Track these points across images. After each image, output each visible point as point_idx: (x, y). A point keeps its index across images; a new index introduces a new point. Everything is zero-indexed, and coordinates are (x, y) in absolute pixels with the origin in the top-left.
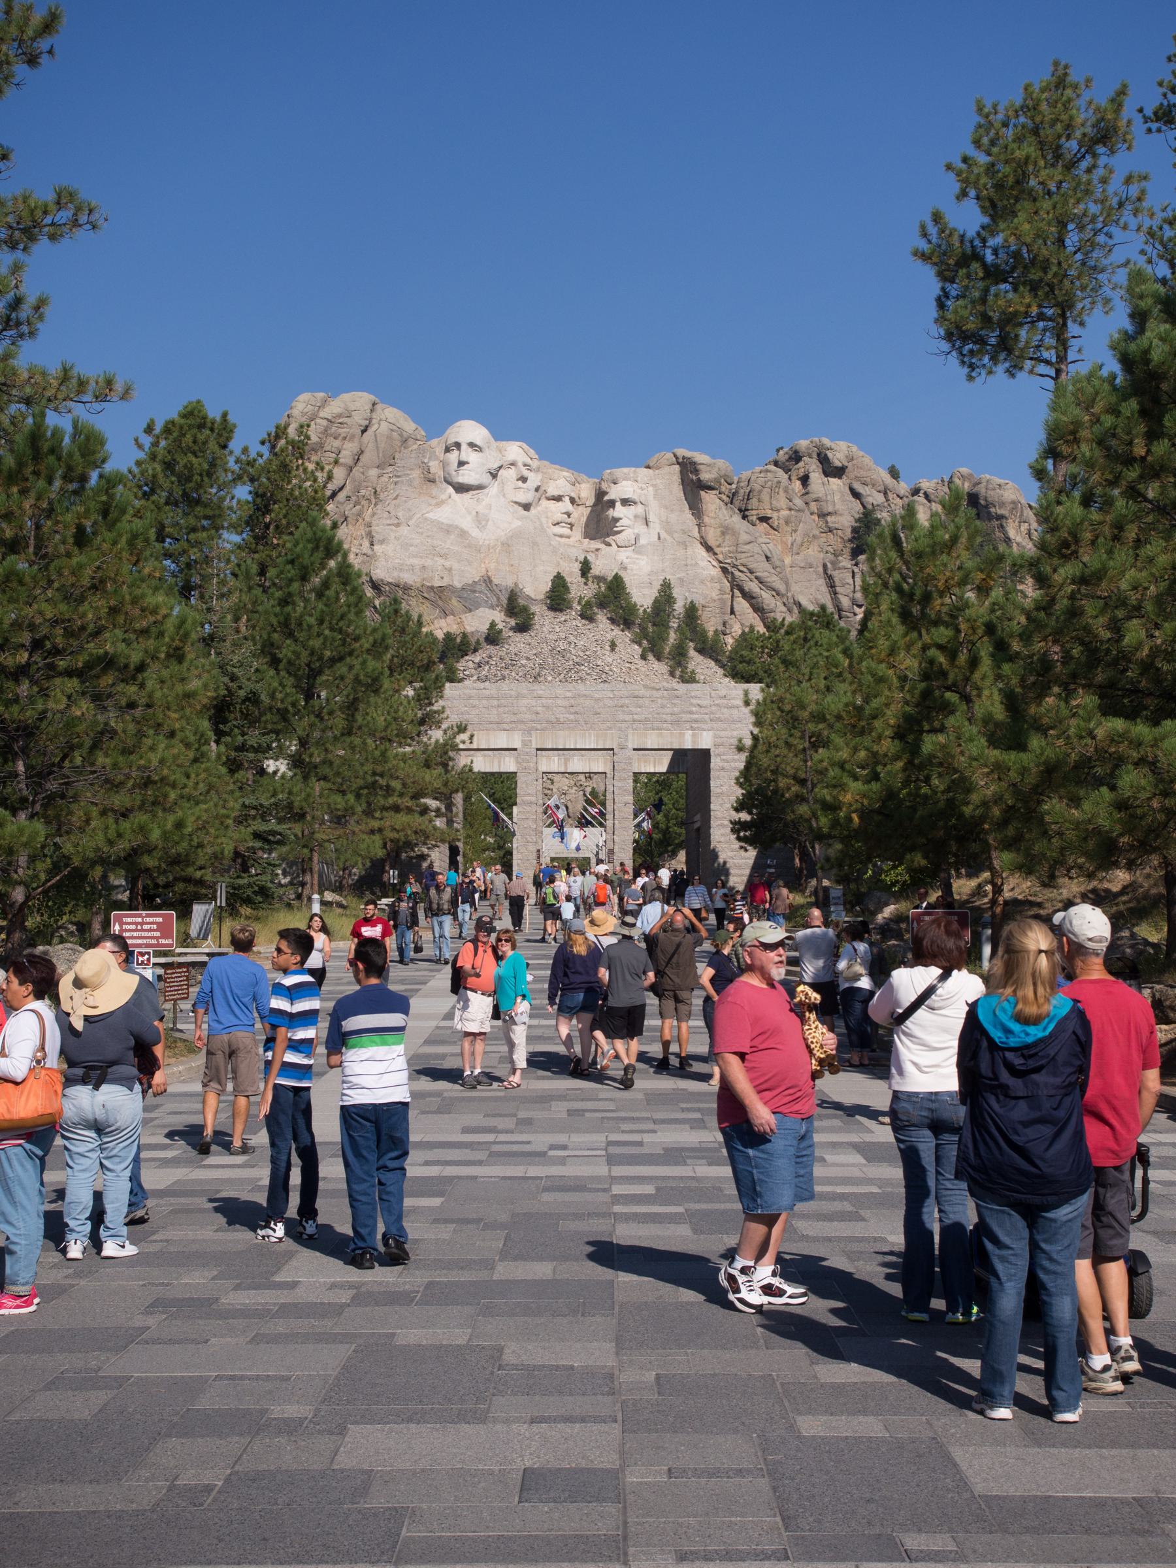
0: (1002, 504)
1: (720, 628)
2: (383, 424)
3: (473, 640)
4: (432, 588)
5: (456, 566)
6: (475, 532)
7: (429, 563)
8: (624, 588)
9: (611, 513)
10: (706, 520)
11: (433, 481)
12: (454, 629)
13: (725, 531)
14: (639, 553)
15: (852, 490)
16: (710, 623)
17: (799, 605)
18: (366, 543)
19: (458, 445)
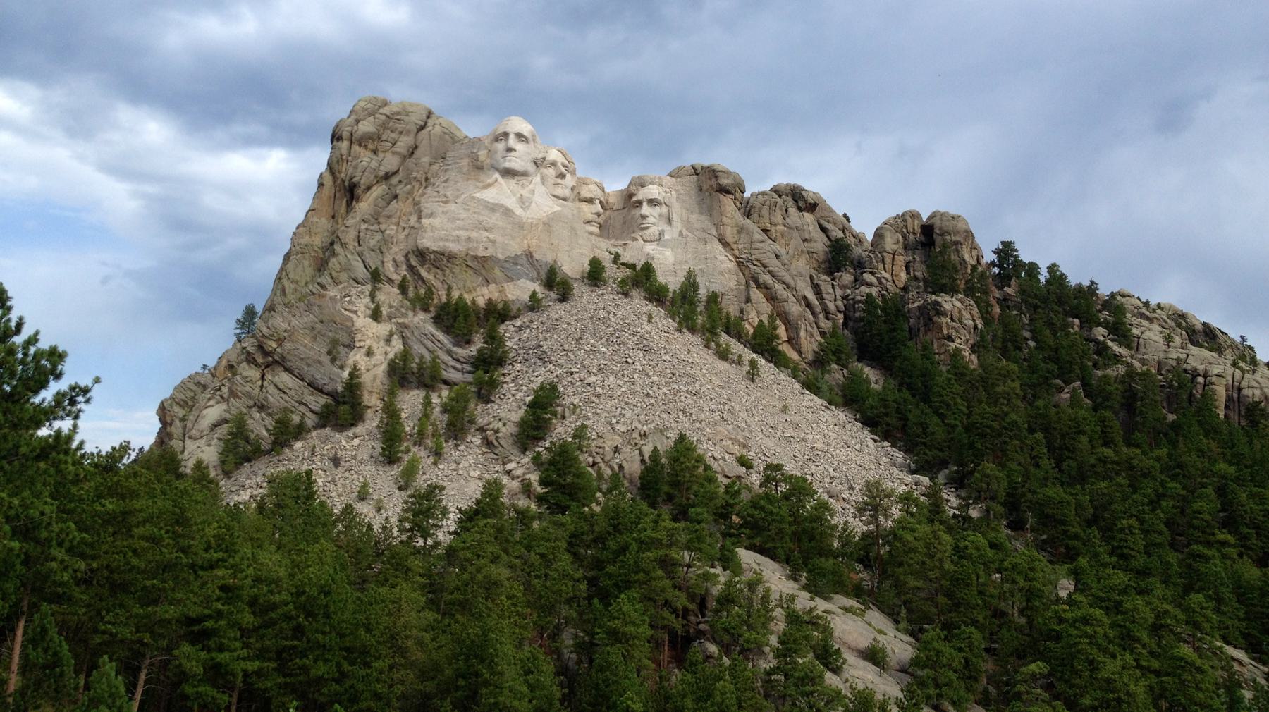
0: (957, 233)
1: (738, 314)
3: (514, 308)
4: (476, 258)
5: (500, 239)
7: (474, 235)
8: (654, 271)
9: (636, 212)
10: (725, 219)
11: (479, 168)
12: (495, 296)
13: (741, 230)
15: (820, 225)
16: (731, 307)
17: (805, 298)
18: (413, 219)
19: (506, 135)
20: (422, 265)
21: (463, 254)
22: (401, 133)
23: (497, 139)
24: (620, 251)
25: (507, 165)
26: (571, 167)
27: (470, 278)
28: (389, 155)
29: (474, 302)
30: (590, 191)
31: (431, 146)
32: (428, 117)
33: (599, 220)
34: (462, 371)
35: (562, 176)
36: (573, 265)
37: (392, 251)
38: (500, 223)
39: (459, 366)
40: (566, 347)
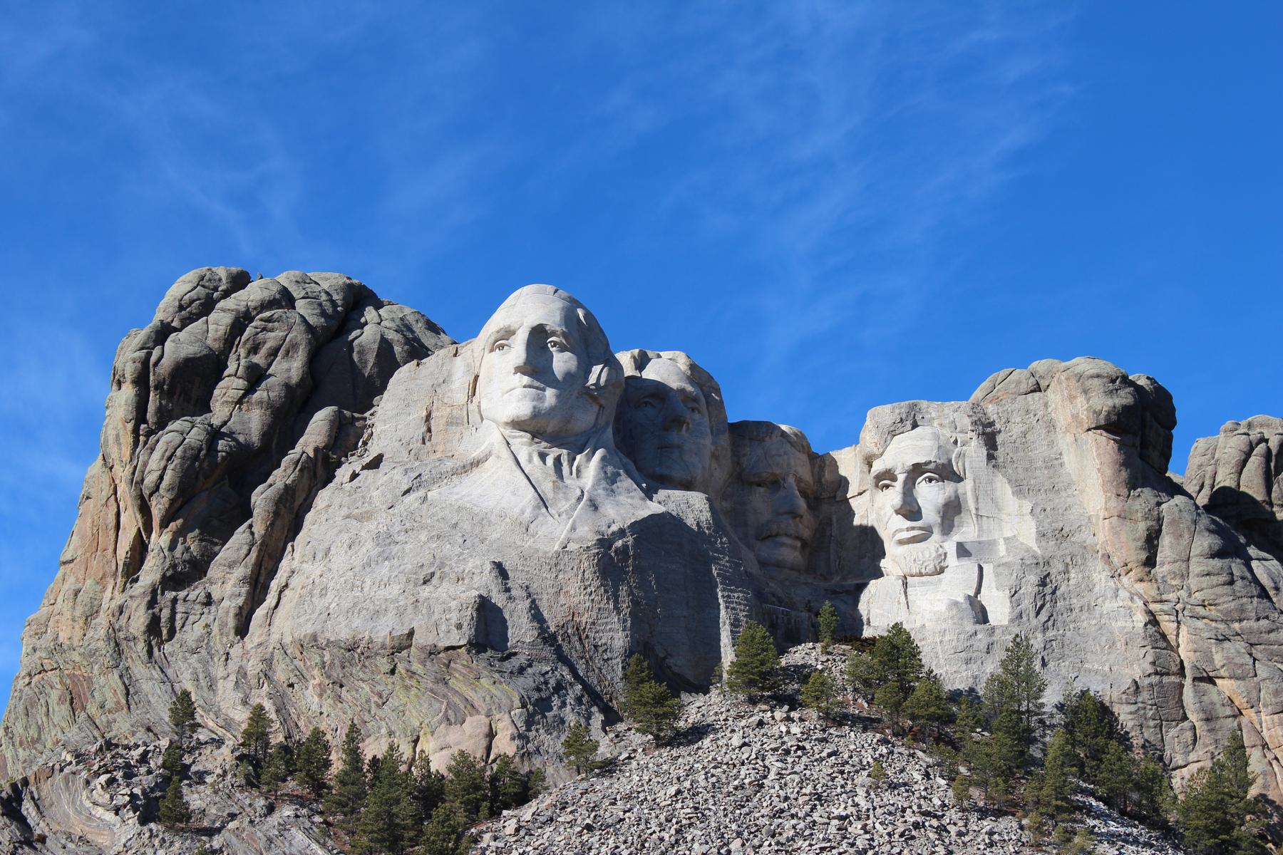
4: (433, 652)
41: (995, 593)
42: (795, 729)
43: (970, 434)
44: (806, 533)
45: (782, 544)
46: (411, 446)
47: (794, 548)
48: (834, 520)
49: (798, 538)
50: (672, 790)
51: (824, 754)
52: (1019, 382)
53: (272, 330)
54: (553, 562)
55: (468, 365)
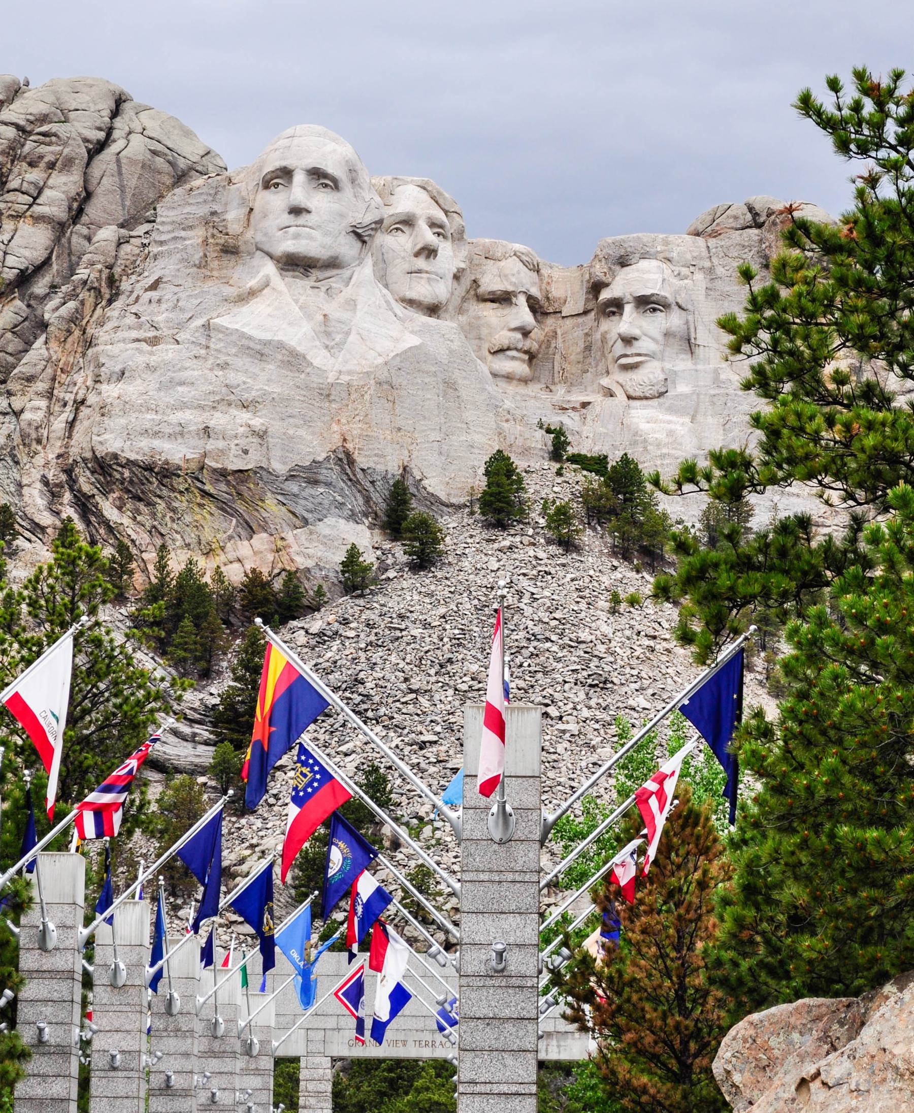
2: (136, 139)
3: (309, 587)
4: (223, 474)
5: (276, 428)
6: (319, 358)
7: (218, 420)
11: (230, 251)
14: (671, 410)
20: (105, 494)
21: (194, 466)
22: (51, 166)
23: (267, 184)
24: (570, 422)
25: (288, 246)
26: (451, 226)
27: (214, 525)
28: (25, 227)
29: (219, 575)
30: (502, 275)
31: (122, 188)
32: (115, 114)
33: (527, 344)
34: (192, 739)
35: (429, 252)
36: (450, 475)
37: (39, 460)
38: (275, 389)
39: (185, 729)
40: (415, 684)
41: (710, 420)
42: (541, 555)
43: (692, 269)
44: (535, 346)
45: (513, 358)
46: (188, 271)
47: (523, 361)
48: (559, 332)
49: (526, 352)
50: (442, 610)
51: (568, 579)
52: (736, 218)
53: (49, 144)
54: (325, 392)
55: (243, 199)
